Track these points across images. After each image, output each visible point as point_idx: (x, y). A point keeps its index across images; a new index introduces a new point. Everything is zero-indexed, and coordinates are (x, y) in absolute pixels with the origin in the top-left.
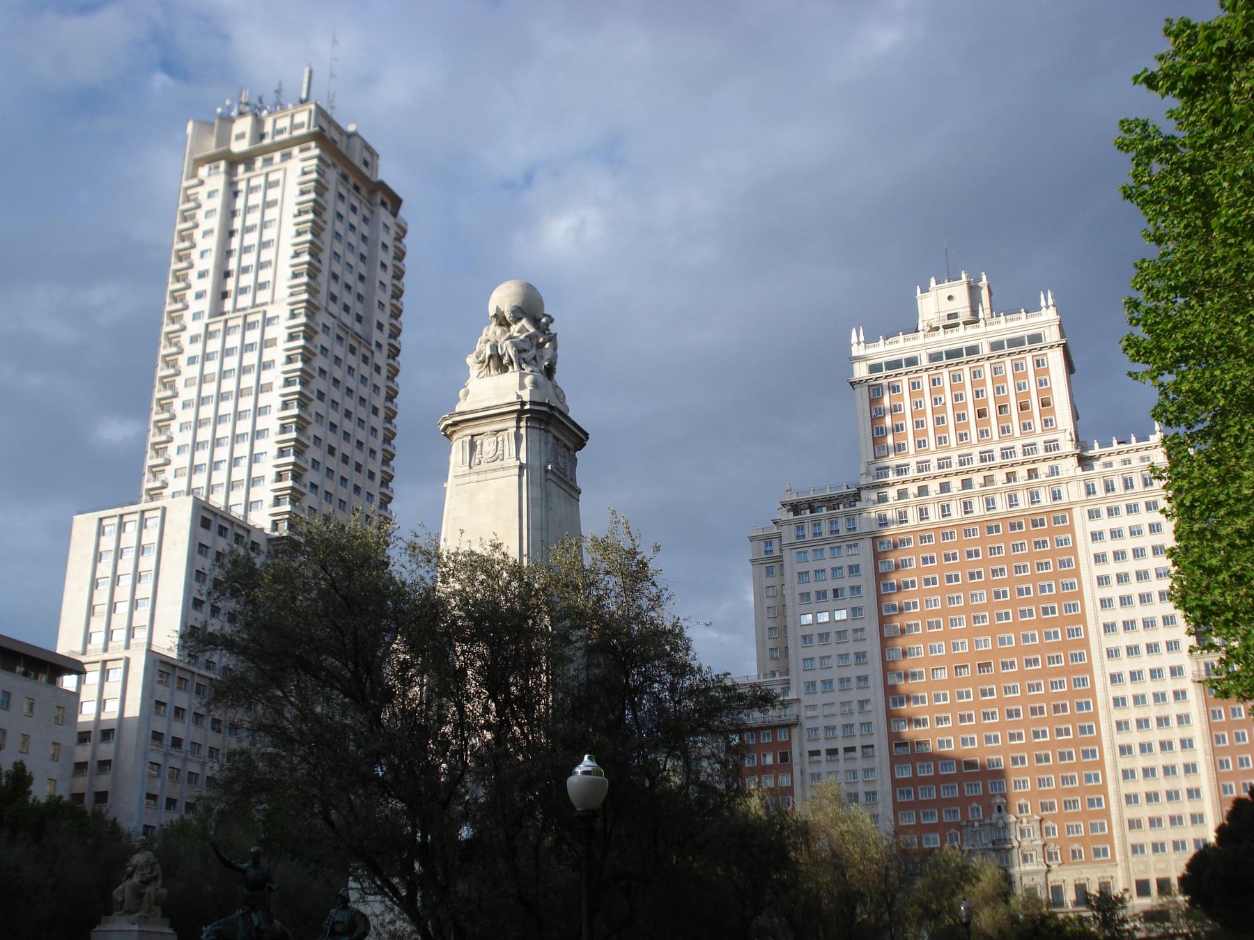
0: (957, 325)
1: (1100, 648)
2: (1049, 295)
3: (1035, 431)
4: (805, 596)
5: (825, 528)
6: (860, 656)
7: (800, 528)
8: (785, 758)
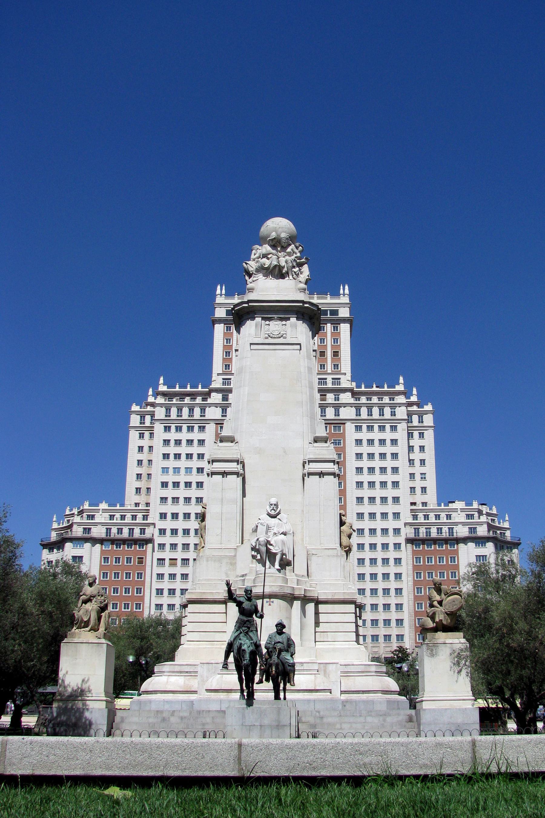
2: (347, 287)
3: (327, 371)
5: (185, 411)
7: (168, 410)
8: (141, 561)
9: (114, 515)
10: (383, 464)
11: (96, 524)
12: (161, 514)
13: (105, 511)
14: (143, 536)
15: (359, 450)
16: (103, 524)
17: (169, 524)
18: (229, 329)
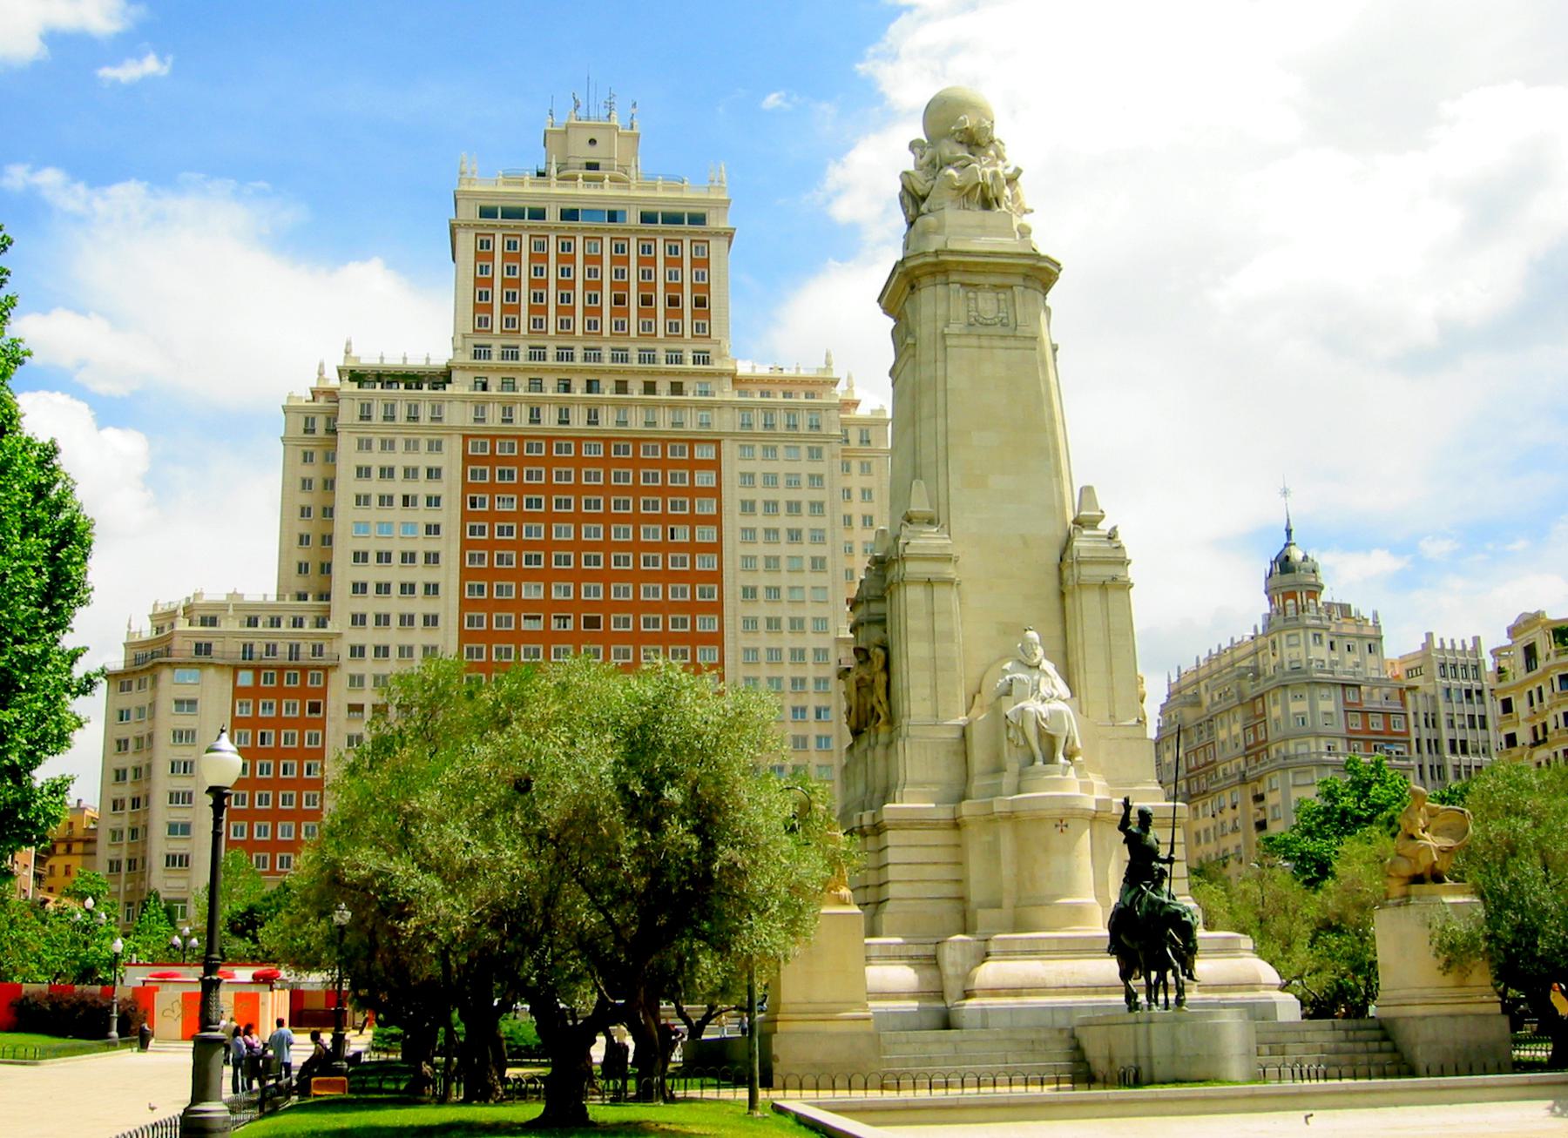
0: (602, 179)
1: (735, 615)
4: (362, 500)
6: (432, 589)
8: (315, 708)
10: (795, 523)
11: (223, 635)
12: (354, 617)
14: (318, 661)
15: (748, 495)
16: (234, 635)
17: (370, 637)
18: (485, 244)
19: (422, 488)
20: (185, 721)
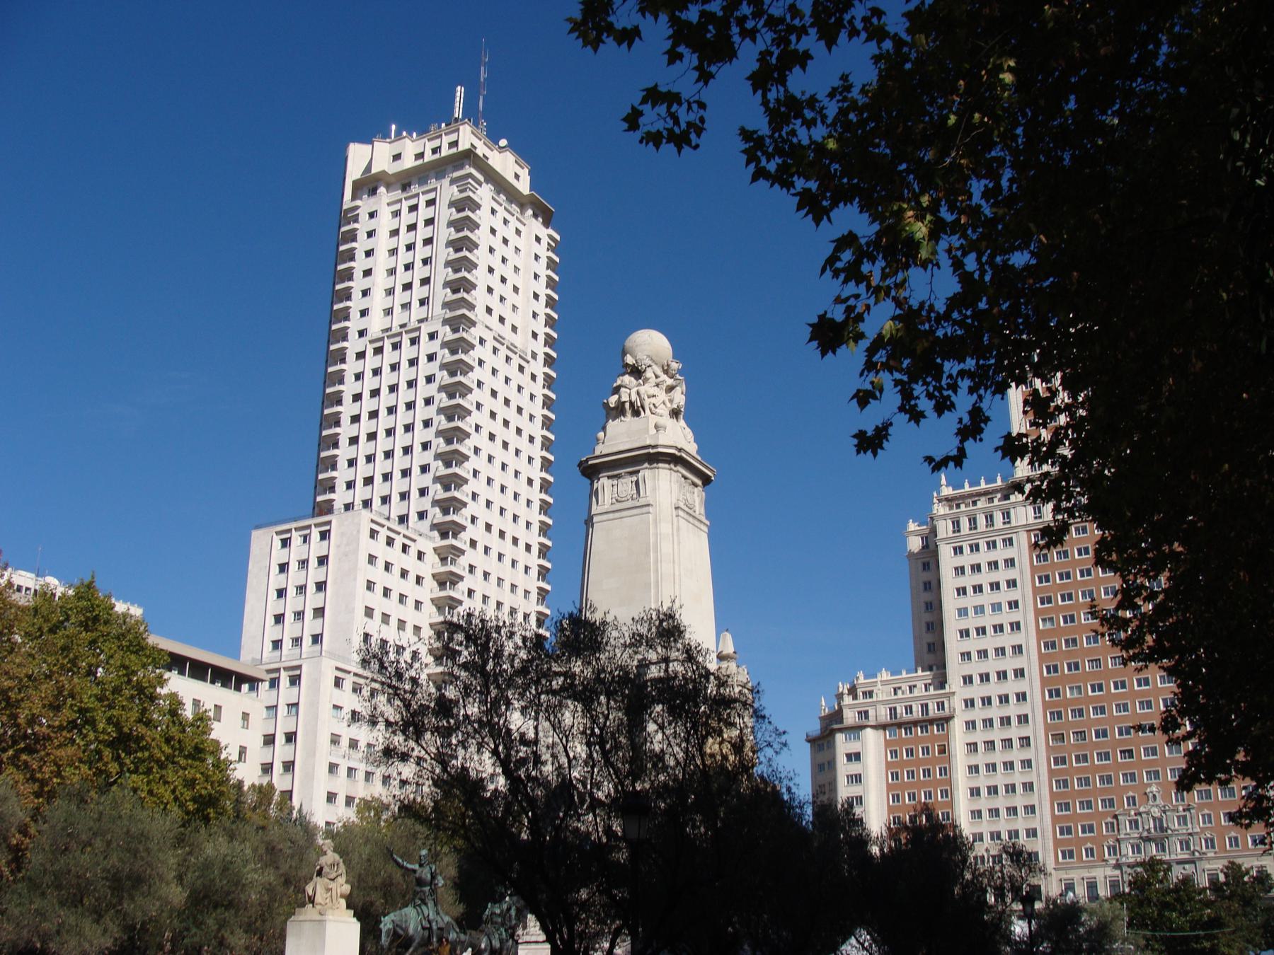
5: (981, 520)
6: (1018, 649)
8: (943, 750)
9: (915, 686)
11: (874, 704)
13: (884, 683)
14: (941, 714)
16: (883, 702)
17: (977, 691)
19: (1002, 575)
20: (854, 768)
